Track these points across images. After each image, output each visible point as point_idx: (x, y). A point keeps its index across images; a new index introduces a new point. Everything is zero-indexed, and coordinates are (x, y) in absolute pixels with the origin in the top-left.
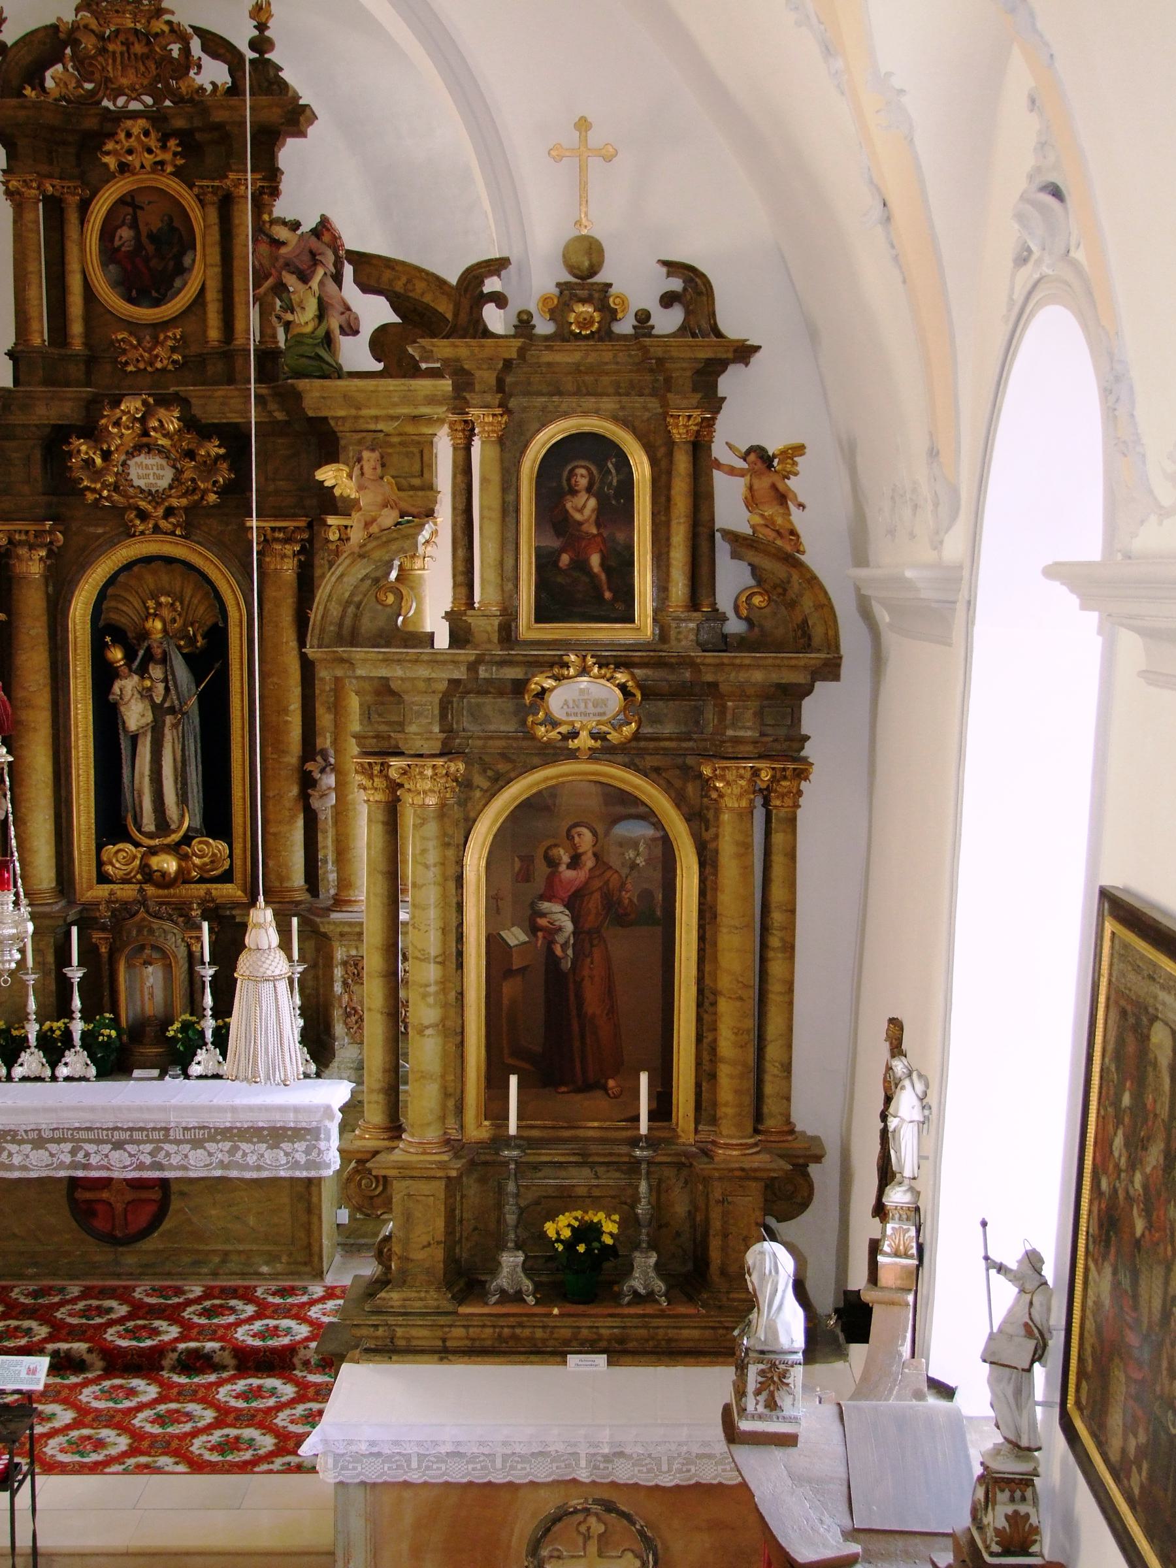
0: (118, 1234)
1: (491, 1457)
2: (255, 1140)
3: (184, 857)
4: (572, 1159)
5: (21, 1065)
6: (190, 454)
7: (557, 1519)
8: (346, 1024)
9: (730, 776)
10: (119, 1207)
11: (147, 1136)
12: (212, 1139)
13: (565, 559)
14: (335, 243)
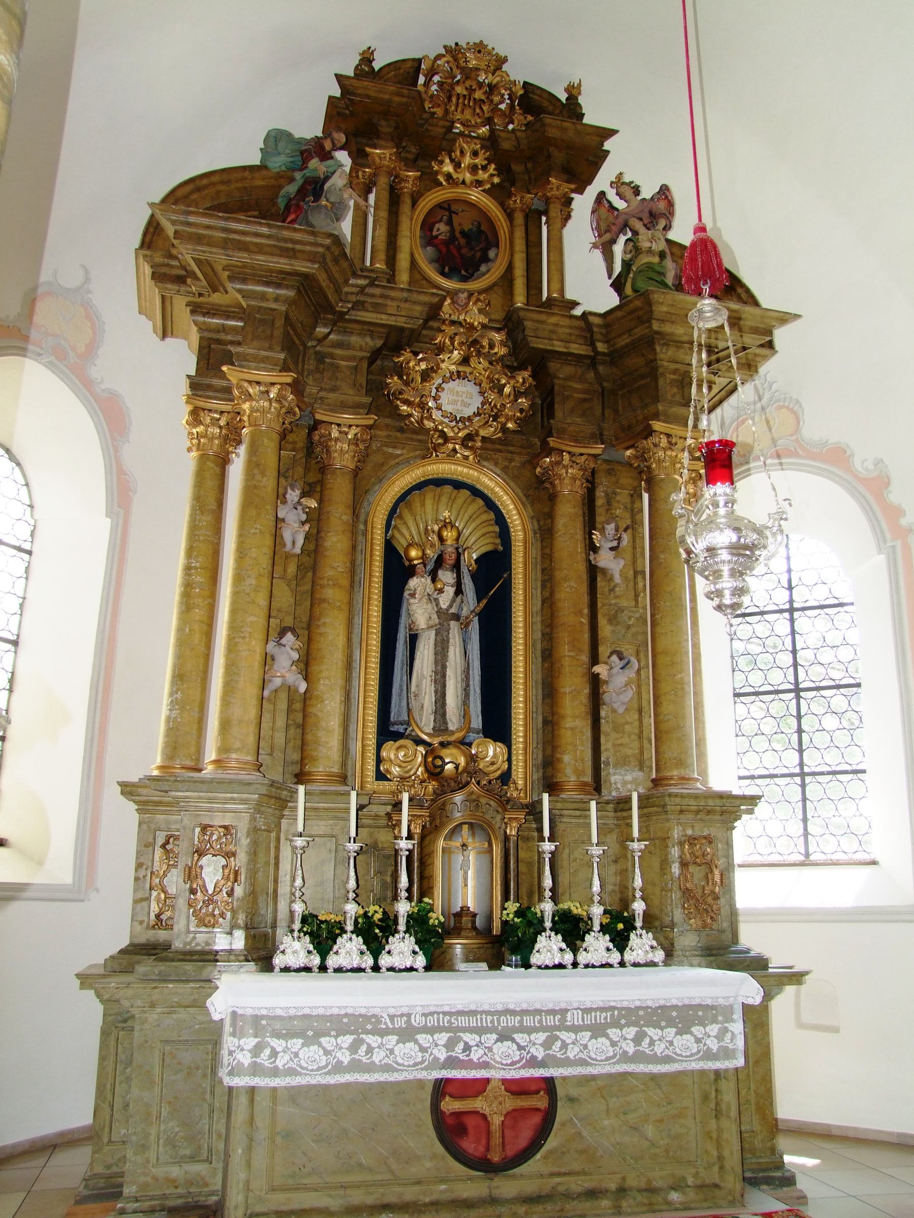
0: (496, 1157)
2: (663, 1024)
5: (337, 953)
10: (496, 1121)
11: (540, 1021)
12: (616, 1024)
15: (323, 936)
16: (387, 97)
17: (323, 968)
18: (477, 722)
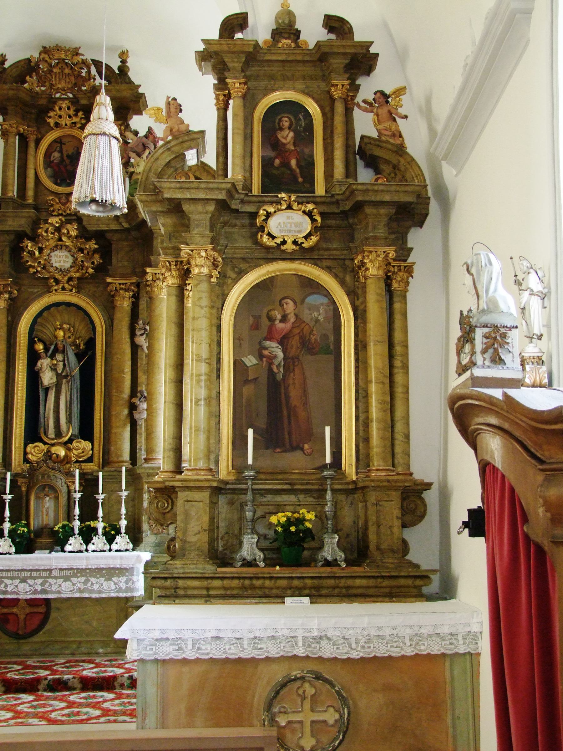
0: (20, 632)
1: (240, 639)
3: (69, 449)
4: (286, 487)
6: (81, 250)
7: (284, 685)
8: (149, 523)
10: (22, 617)
12: (75, 576)
13: (277, 162)
16: (5, 92)
18: (76, 432)
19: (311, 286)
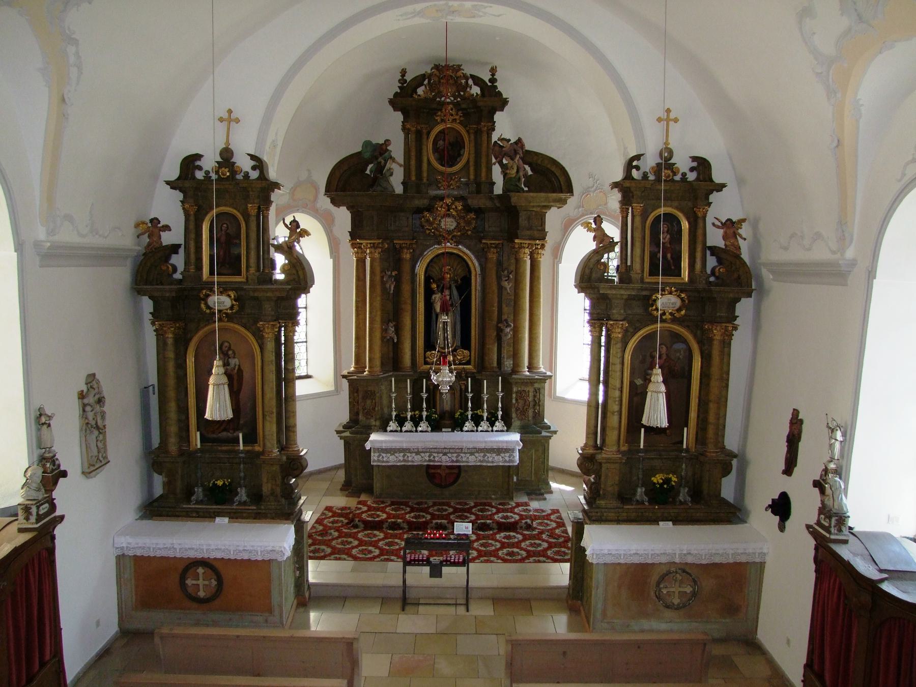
1: (647, 555)
9: (718, 328)
14: (523, 146)
15: (401, 421)
17: (401, 431)
19: (677, 337)
